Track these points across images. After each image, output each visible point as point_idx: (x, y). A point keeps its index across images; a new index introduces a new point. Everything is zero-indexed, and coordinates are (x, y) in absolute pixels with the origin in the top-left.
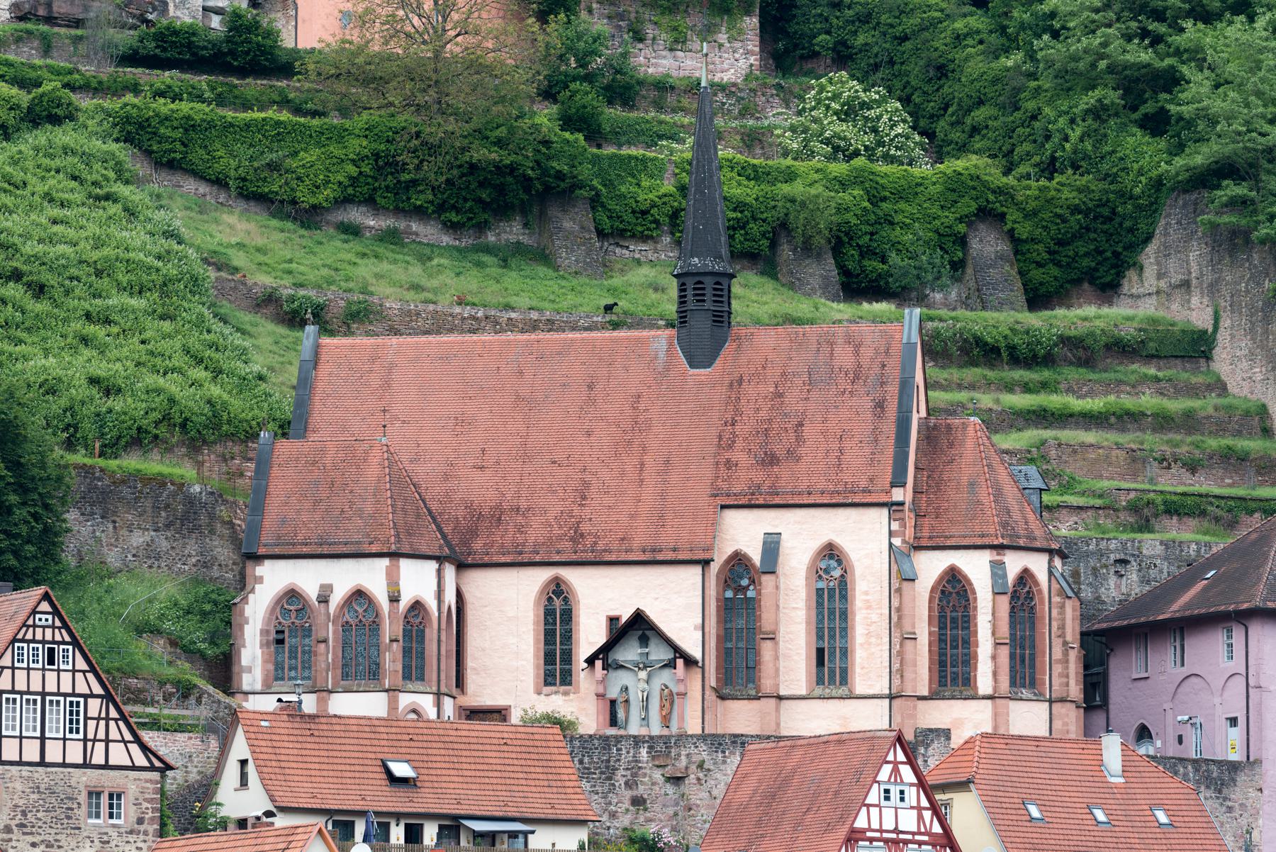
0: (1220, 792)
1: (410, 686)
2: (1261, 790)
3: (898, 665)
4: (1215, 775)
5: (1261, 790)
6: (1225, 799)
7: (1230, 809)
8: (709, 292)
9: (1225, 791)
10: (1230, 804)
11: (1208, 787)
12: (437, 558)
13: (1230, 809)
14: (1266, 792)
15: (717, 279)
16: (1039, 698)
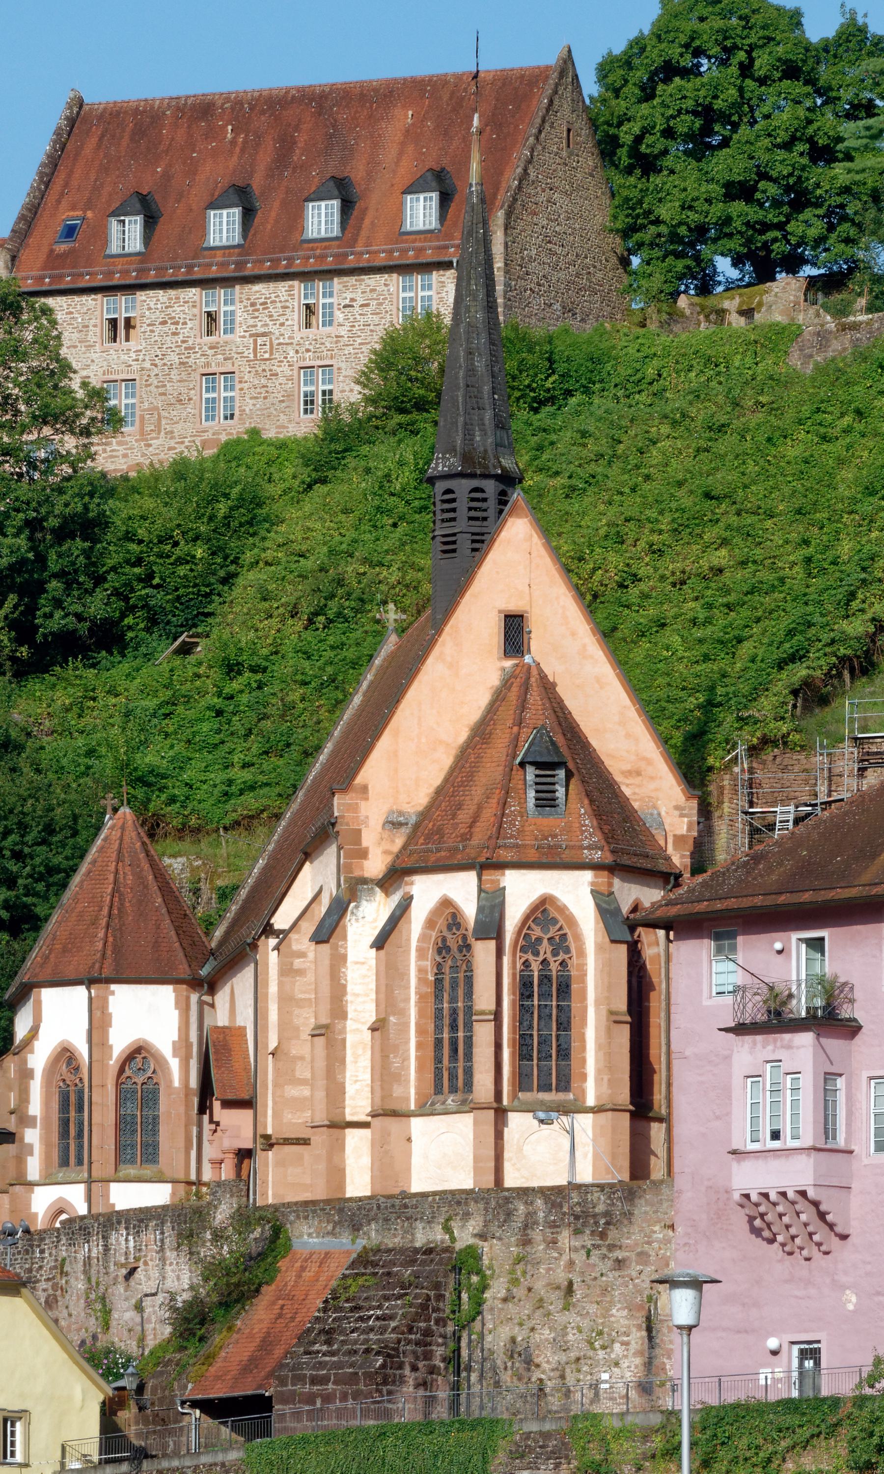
0: (603, 1235)
1: (132, 1171)
2: (672, 1227)
3: (385, 1073)
4: (601, 1208)
5: (672, 1227)
6: (611, 1247)
7: (620, 1264)
8: (462, 505)
9: (613, 1233)
10: (619, 1254)
11: (577, 1232)
12: (90, 982)
13: (620, 1264)
14: (679, 1229)
15: (475, 483)
16: (467, 1106)
